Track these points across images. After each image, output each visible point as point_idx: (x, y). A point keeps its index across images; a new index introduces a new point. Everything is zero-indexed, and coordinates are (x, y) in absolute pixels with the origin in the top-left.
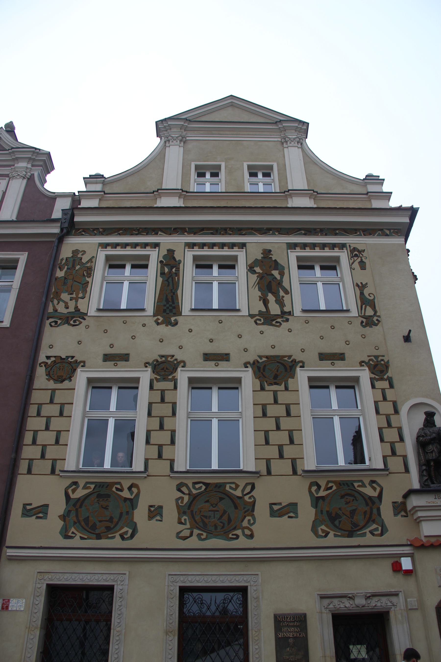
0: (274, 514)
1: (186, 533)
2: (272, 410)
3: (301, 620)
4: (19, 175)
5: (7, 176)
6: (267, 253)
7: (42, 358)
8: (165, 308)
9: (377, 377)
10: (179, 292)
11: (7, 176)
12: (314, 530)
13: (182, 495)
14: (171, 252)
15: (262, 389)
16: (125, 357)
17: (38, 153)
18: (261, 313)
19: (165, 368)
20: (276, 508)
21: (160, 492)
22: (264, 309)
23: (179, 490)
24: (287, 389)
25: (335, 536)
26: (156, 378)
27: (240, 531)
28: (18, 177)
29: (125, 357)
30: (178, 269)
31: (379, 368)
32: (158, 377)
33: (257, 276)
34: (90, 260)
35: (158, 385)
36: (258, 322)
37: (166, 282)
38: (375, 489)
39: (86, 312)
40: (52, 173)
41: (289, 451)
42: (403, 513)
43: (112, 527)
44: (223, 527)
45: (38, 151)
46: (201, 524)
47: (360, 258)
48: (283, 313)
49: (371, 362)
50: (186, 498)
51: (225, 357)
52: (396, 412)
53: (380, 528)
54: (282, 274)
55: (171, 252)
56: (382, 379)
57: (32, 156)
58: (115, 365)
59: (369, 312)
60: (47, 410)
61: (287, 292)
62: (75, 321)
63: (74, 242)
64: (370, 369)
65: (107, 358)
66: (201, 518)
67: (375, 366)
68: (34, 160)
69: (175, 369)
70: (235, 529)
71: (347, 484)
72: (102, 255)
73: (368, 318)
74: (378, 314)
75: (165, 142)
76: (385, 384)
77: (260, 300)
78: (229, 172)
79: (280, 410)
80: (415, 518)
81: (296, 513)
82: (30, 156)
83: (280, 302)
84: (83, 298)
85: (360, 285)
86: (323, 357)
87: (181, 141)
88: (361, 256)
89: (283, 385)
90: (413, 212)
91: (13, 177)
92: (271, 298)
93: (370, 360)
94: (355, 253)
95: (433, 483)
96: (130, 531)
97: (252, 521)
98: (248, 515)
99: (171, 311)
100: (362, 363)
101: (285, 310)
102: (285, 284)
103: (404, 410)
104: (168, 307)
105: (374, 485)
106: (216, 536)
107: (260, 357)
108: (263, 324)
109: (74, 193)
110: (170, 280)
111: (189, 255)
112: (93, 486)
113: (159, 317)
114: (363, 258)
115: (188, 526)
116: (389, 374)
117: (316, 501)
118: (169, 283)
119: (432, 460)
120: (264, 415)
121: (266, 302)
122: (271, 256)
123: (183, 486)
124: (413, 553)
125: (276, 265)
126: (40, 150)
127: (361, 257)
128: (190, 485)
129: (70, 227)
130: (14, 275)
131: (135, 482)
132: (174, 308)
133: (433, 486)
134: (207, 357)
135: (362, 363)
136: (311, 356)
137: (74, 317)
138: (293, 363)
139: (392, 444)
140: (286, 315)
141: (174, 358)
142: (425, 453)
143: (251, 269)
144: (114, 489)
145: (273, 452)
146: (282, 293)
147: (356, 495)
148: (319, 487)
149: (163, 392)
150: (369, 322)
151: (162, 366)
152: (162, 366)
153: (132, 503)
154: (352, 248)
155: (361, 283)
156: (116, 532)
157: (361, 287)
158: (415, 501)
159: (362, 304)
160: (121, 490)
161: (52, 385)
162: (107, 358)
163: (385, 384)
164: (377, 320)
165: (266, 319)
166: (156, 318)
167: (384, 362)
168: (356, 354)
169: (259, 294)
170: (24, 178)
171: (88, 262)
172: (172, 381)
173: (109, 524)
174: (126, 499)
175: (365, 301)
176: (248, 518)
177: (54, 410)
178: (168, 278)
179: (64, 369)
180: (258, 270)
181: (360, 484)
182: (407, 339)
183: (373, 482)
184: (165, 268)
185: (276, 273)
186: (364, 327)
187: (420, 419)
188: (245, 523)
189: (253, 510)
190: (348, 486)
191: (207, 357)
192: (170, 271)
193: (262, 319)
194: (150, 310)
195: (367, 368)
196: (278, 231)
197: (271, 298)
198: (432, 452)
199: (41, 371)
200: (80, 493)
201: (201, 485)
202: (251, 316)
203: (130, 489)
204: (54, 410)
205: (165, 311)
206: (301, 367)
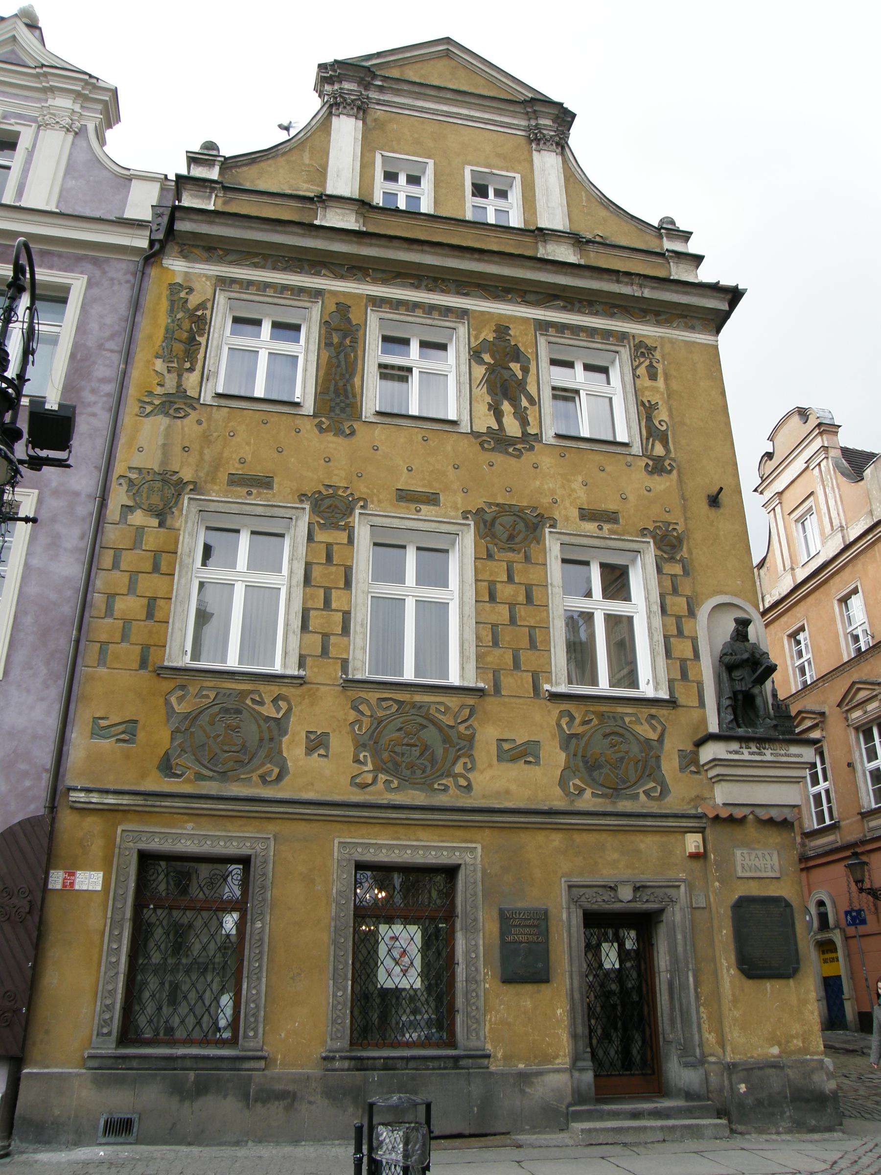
1: (369, 778)
2: (505, 591)
3: (540, 921)
4: (58, 122)
5: (34, 120)
6: (502, 330)
8: (333, 404)
9: (666, 556)
10: (357, 380)
11: (34, 120)
12: (563, 783)
13: (360, 717)
15: (490, 556)
17: (94, 87)
20: (506, 746)
22: (495, 426)
23: (355, 708)
24: (527, 559)
25: (594, 795)
26: (318, 522)
27: (451, 779)
28: (57, 127)
30: (355, 341)
32: (322, 522)
33: (487, 369)
34: (202, 306)
35: (321, 536)
36: (486, 446)
37: (334, 361)
38: (654, 728)
39: (196, 396)
40: (116, 128)
42: (693, 769)
43: (246, 761)
44: (424, 772)
45: (94, 81)
46: (390, 765)
47: (648, 361)
48: (525, 434)
49: (658, 531)
50: (366, 721)
52: (692, 613)
53: (659, 788)
54: (525, 370)
55: (343, 309)
56: (672, 559)
57: (83, 88)
58: (249, 494)
59: (659, 450)
61: (532, 401)
62: (177, 410)
64: (655, 543)
66: (391, 756)
67: (664, 537)
68: (86, 98)
69: (351, 512)
70: (441, 776)
71: (614, 717)
73: (658, 460)
74: (673, 455)
75: (331, 106)
76: (677, 569)
77: (489, 410)
80: (709, 776)
81: (537, 757)
82: (80, 89)
83: (522, 417)
84: (191, 370)
85: (647, 405)
87: (359, 108)
88: (651, 356)
89: (522, 555)
90: (734, 295)
91: (47, 124)
92: (506, 407)
93: (656, 528)
95: (739, 727)
96: (276, 771)
97: (469, 766)
98: (464, 755)
99: (343, 410)
100: (644, 532)
101: (529, 432)
102: (532, 388)
103: (703, 612)
105: (653, 722)
106: (415, 785)
107: (490, 504)
108: (493, 450)
109: (166, 176)
110: (342, 356)
112: (212, 695)
113: (323, 419)
114: (653, 361)
115: (370, 767)
116: (684, 553)
117: (567, 741)
118: (339, 362)
119: (741, 691)
120: (492, 597)
122: (508, 338)
123: (362, 703)
124: (705, 828)
125: (516, 354)
126: (98, 79)
127: (650, 359)
128: (373, 702)
130: (63, 313)
131: (284, 691)
132: (348, 405)
133: (741, 731)
135: (644, 532)
137: (175, 403)
138: (539, 519)
139: (683, 661)
141: (349, 492)
142: (731, 679)
143: (475, 355)
144: (249, 702)
146: (524, 403)
147: (628, 735)
148: (572, 718)
149: (329, 547)
151: (327, 502)
152: (327, 502)
153: (280, 726)
154: (637, 341)
155: (649, 401)
156: (253, 771)
158: (708, 752)
159: (650, 434)
160: (261, 703)
163: (677, 569)
164: (670, 464)
166: (317, 420)
167: (677, 533)
169: (489, 399)
170: (68, 130)
171: (197, 308)
172: (345, 530)
173: (241, 756)
174: (268, 719)
175: (652, 432)
176: (462, 760)
178: (338, 354)
180: (487, 358)
181: (634, 719)
182: (714, 501)
183: (652, 717)
184: (334, 335)
185: (515, 367)
186: (651, 473)
188: (458, 768)
189: (471, 747)
190: (616, 721)
192: (341, 344)
193: (492, 443)
194: (309, 407)
195: (651, 541)
196: (520, 296)
197: (506, 407)
198: (741, 680)
201: (391, 703)
202: (475, 434)
203: (275, 701)
205: (332, 409)
206: (551, 526)
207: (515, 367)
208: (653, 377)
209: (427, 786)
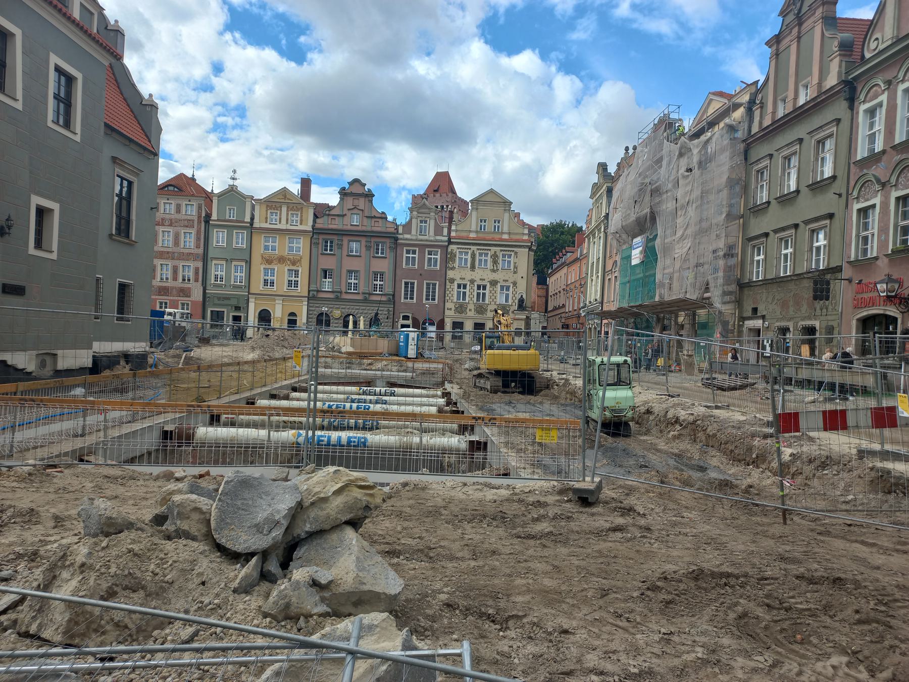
21: (471, 306)
63: (452, 247)
94: (516, 253)
104: (473, 267)
129: (450, 242)
136: (501, 281)
150: (515, 273)
165: (493, 271)
175: (515, 267)
179: (452, 281)
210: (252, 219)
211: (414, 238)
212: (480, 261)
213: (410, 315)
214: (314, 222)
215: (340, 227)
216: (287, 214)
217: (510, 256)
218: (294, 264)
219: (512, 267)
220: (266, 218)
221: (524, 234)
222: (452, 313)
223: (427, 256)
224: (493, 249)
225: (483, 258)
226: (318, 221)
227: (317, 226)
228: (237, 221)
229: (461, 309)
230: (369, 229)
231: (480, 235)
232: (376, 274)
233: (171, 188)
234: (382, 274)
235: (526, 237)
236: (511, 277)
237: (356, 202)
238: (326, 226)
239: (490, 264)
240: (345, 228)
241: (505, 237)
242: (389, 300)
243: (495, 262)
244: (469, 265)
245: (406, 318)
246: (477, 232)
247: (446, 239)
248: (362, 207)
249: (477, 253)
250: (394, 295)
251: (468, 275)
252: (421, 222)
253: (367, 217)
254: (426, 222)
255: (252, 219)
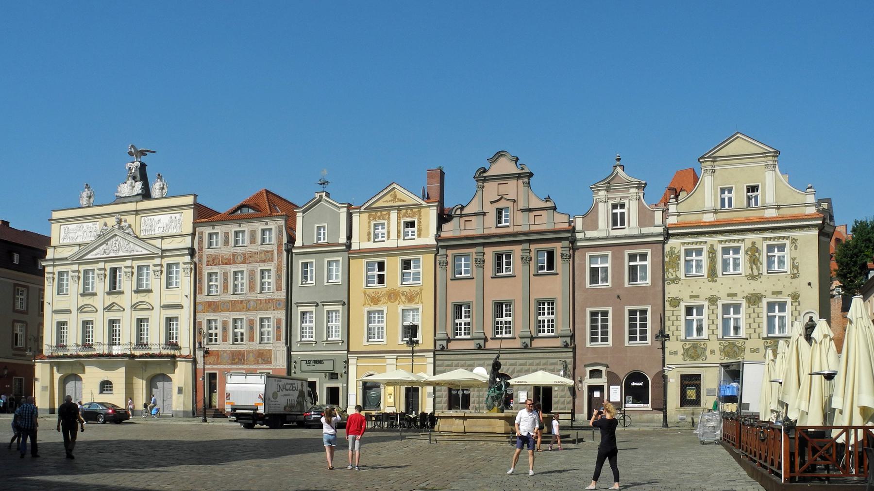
0: (751, 351)
2: (753, 316)
5: (627, 197)
6: (754, 243)
7: (666, 298)
11: (627, 197)
14: (712, 246)
16: (698, 296)
18: (750, 275)
19: (713, 300)
29: (698, 296)
31: (795, 297)
41: (758, 330)
51: (735, 295)
55: (712, 246)
59: (795, 272)
60: (672, 318)
65: (691, 297)
72: (683, 248)
78: (736, 192)
79: (755, 315)
83: (758, 269)
86: (773, 293)
92: (754, 267)
94: (794, 241)
102: (761, 260)
111: (720, 246)
121: (752, 269)
125: (757, 250)
129: (668, 236)
134: (729, 295)
136: (769, 293)
140: (760, 274)
145: (752, 331)
150: (794, 276)
153: (705, 349)
157: (794, 259)
161: (672, 309)
162: (691, 297)
165: (752, 277)
168: (788, 291)
175: (795, 267)
177: (674, 318)
179: (675, 302)
185: (757, 254)
187: (807, 319)
191: (729, 295)
194: (706, 276)
197: (754, 267)
199: (667, 304)
200: (687, 347)
204: (674, 318)
207: (757, 254)
208: (796, 249)
209: (735, 358)
210: (349, 237)
211: (604, 235)
212: (725, 263)
213: (603, 369)
214: (439, 228)
215: (479, 232)
216: (398, 224)
217: (781, 248)
218: (411, 299)
219: (787, 267)
220: (369, 234)
221: (807, 205)
222: (679, 359)
223: (626, 263)
224: (749, 237)
225: (731, 256)
226: (445, 227)
227: (443, 235)
228: (328, 245)
229: (694, 351)
230: (525, 229)
231: (722, 216)
232: (540, 303)
233: (245, 210)
234: (551, 302)
235: (812, 210)
236: (786, 285)
237: (503, 189)
238: (457, 234)
239: (744, 267)
240: (487, 232)
241: (771, 213)
242: (566, 346)
243: (754, 261)
244: (705, 271)
245: (595, 374)
246: (716, 212)
247: (660, 230)
248: (512, 196)
249: (719, 249)
250: (573, 337)
251: (705, 288)
252: (614, 207)
253: (523, 210)
254: (622, 206)
255: (349, 237)
